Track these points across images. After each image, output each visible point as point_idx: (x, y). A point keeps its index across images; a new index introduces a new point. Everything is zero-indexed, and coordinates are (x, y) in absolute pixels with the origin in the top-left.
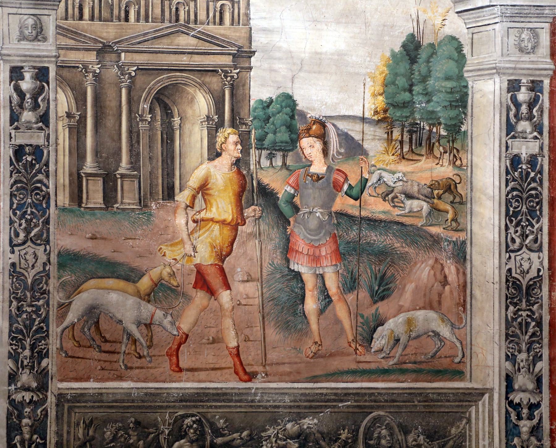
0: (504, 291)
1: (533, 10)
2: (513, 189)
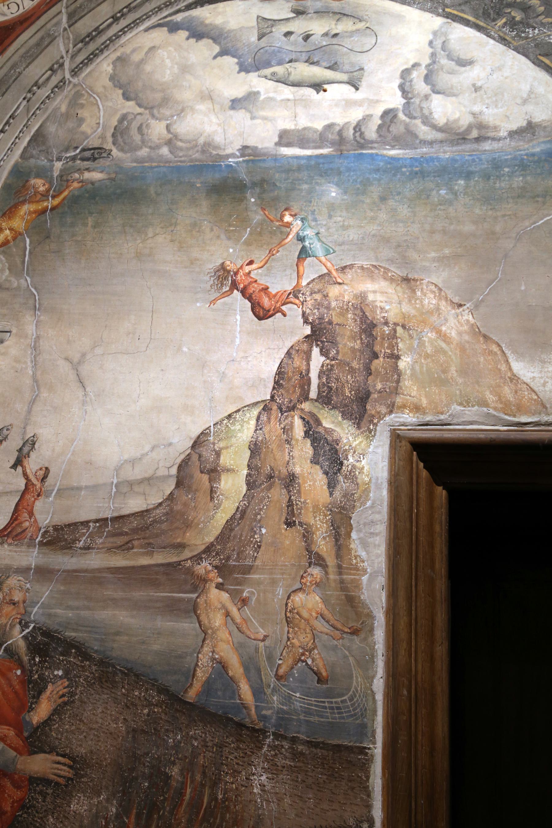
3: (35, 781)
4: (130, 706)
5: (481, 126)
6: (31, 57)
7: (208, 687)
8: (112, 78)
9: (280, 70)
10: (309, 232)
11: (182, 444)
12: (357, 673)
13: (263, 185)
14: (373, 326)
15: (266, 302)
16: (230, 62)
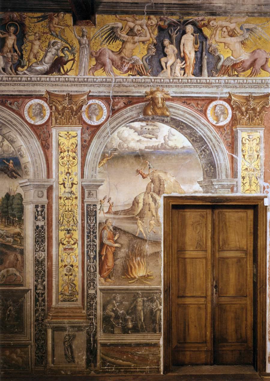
0: (34, 263)
1: (42, 186)
2: (37, 235)
3: (116, 247)
4: (128, 237)
5: (176, 147)
6: (103, 131)
7: (139, 234)
8: (117, 136)
9: (144, 135)
10: (150, 164)
11: (133, 199)
12: (159, 232)
13: (143, 156)
14: (160, 180)
15: (144, 176)
16: (136, 133)
